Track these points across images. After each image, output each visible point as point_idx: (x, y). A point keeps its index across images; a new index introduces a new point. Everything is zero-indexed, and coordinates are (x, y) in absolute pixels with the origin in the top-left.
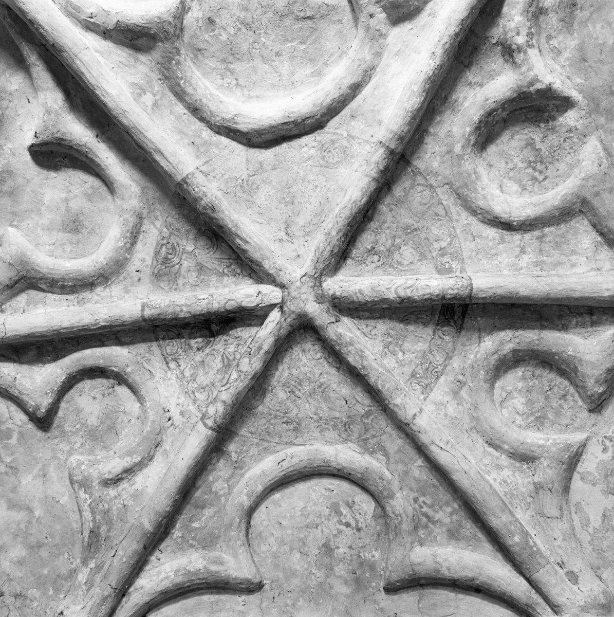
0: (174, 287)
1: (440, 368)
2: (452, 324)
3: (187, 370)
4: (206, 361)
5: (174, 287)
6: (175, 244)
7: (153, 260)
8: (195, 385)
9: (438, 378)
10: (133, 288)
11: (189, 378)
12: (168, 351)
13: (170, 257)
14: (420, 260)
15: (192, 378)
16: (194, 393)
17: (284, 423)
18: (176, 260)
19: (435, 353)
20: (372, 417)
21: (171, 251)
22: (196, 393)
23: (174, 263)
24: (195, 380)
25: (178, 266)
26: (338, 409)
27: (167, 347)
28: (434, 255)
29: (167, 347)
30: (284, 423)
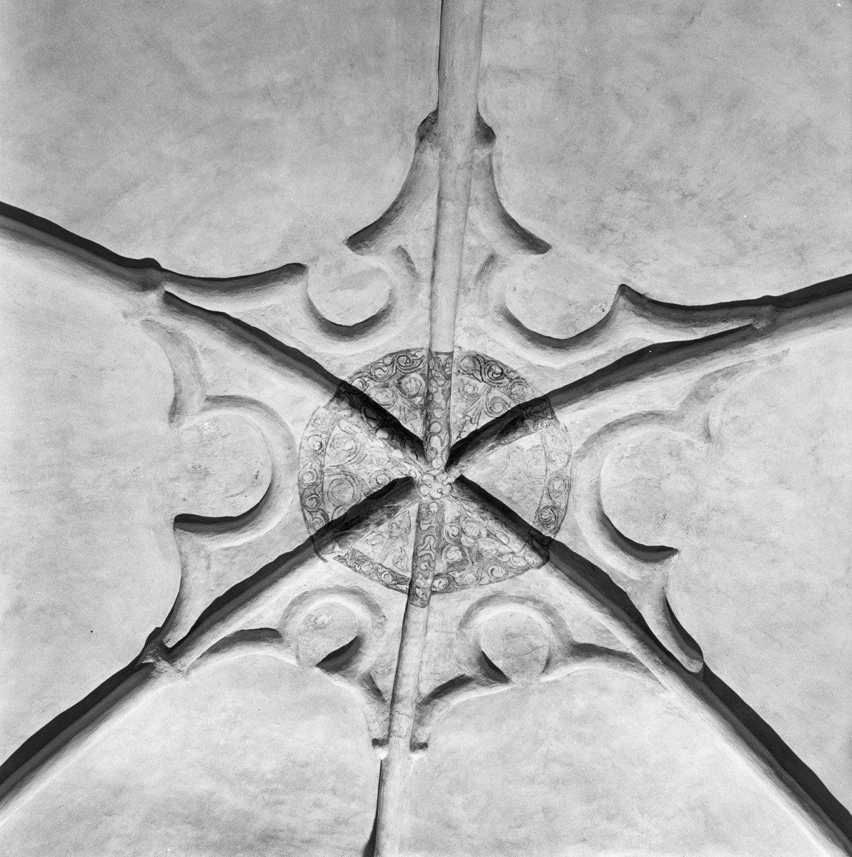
0: (461, 371)
1: (358, 569)
2: (393, 582)
3: (382, 373)
4: (387, 389)
5: (461, 371)
6: (500, 381)
7: (491, 358)
8: (366, 379)
9: (350, 567)
10: (468, 334)
11: (373, 374)
12: (402, 358)
13: (490, 373)
14: (448, 563)
15: (373, 377)
16: (360, 377)
17: (321, 444)
18: (486, 378)
19: (371, 566)
20: (322, 519)
21: (495, 376)
22: (359, 379)
23: (483, 375)
24: (372, 379)
25: (480, 378)
26: (330, 490)
27: (406, 358)
28: (450, 573)
29: (406, 358)
30: (321, 444)
